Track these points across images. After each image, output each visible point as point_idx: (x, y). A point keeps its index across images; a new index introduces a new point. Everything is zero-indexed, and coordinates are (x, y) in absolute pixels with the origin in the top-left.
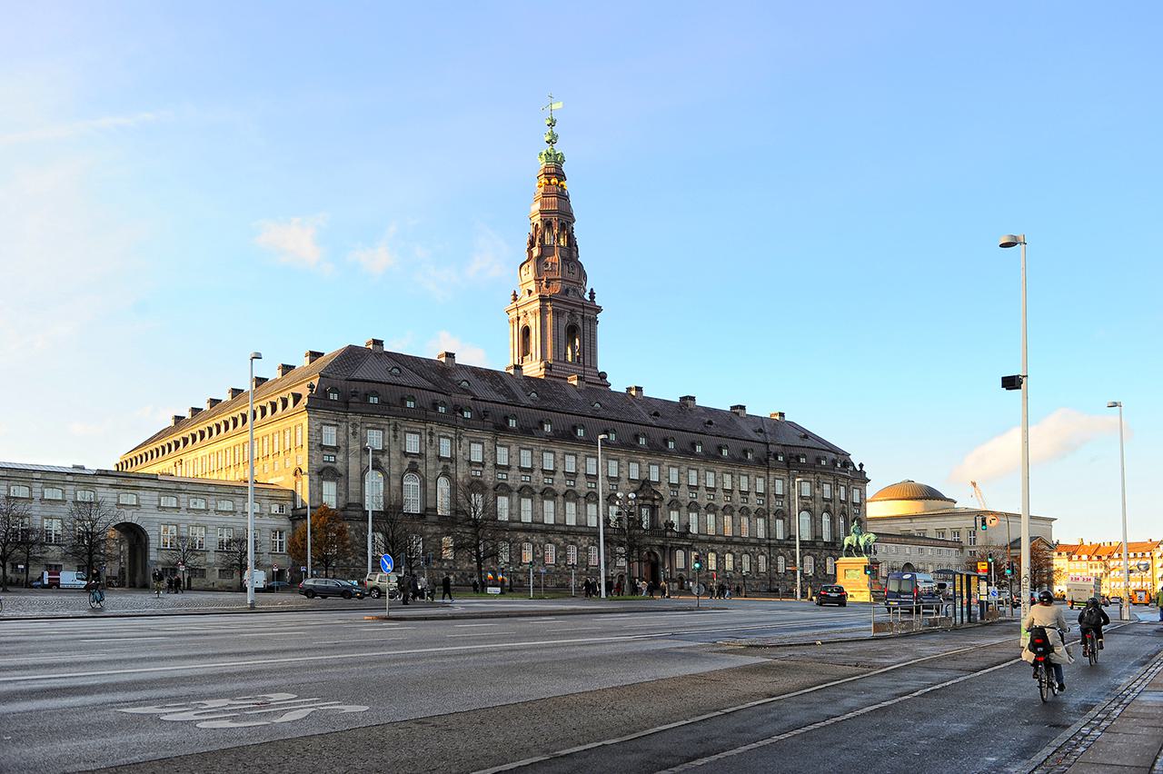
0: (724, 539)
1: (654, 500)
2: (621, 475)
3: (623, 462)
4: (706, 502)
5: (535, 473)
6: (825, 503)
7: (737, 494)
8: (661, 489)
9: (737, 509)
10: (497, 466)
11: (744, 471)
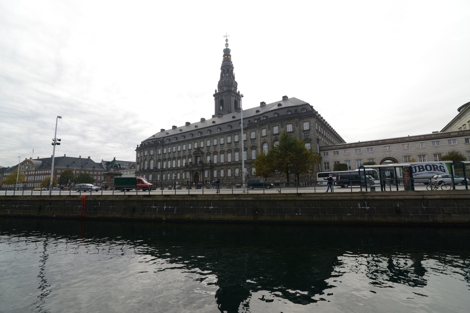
0: (227, 163)
3: (193, 143)
4: (220, 150)
6: (274, 137)
7: (233, 144)
9: (233, 150)
10: (164, 154)
11: (236, 133)
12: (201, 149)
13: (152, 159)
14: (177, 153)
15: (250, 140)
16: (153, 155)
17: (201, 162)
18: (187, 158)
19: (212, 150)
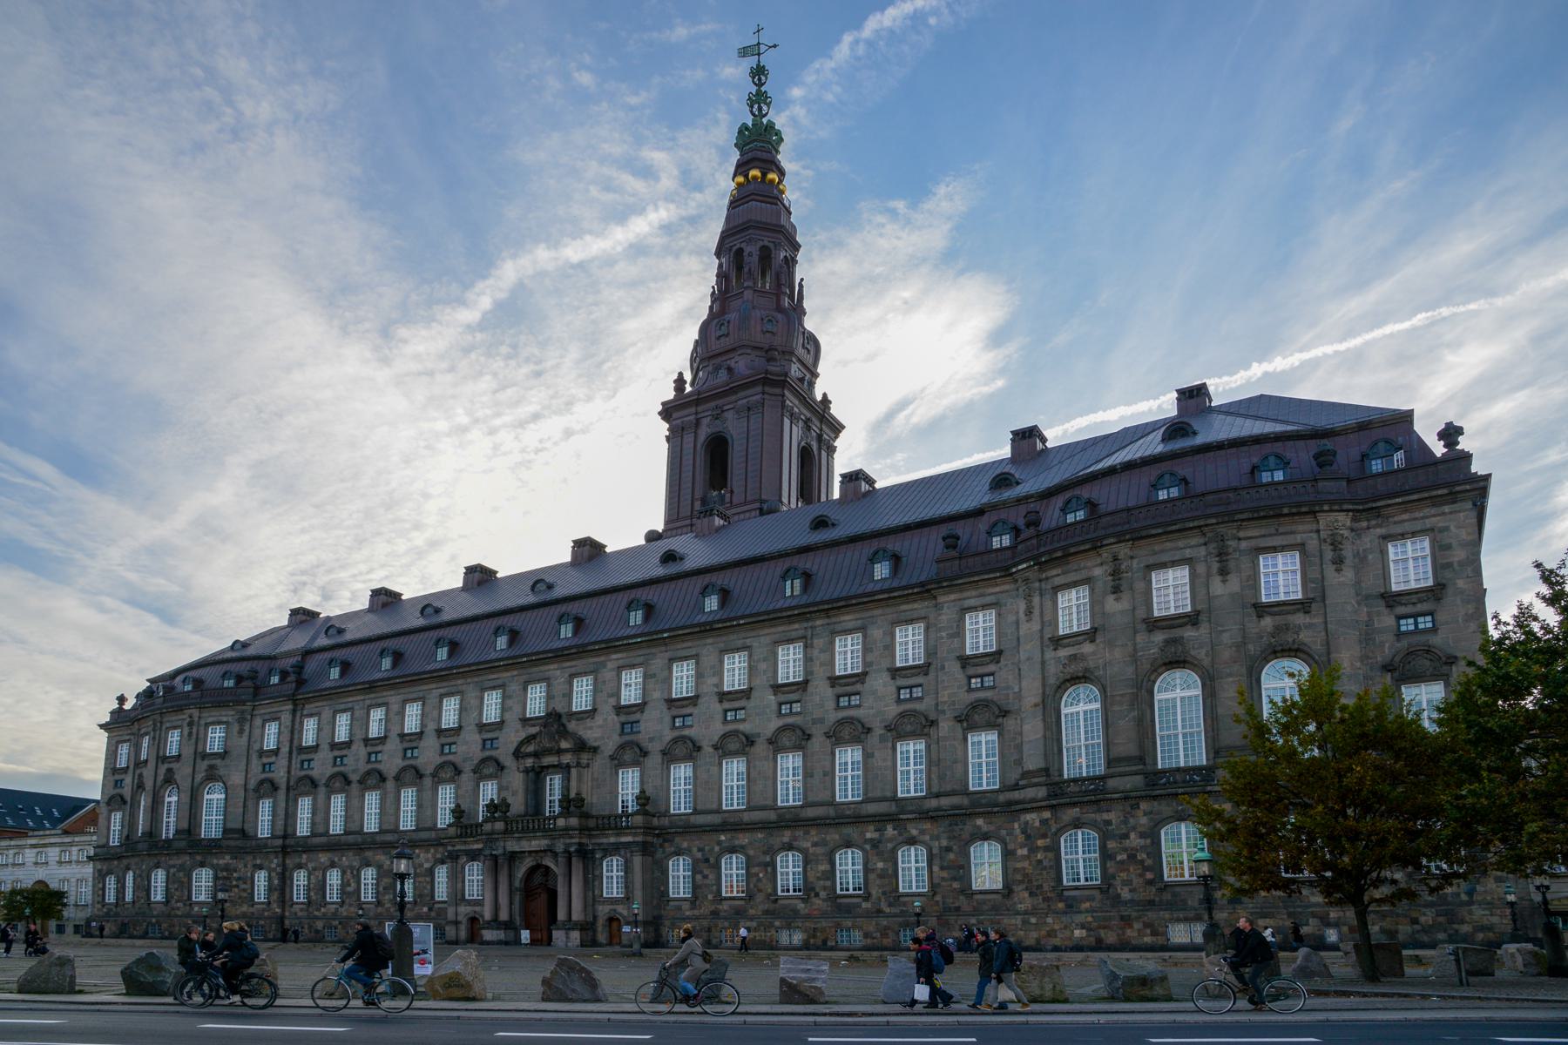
1: (560, 752)
2: (507, 716)
4: (718, 729)
5: (354, 747)
7: (821, 692)
8: (590, 733)
9: (818, 732)
10: (301, 750)
11: (848, 619)
12: (572, 726)
13: (212, 776)
14: (393, 745)
15: (954, 668)
16: (223, 755)
17: (571, 804)
18: (467, 777)
19: (655, 728)
